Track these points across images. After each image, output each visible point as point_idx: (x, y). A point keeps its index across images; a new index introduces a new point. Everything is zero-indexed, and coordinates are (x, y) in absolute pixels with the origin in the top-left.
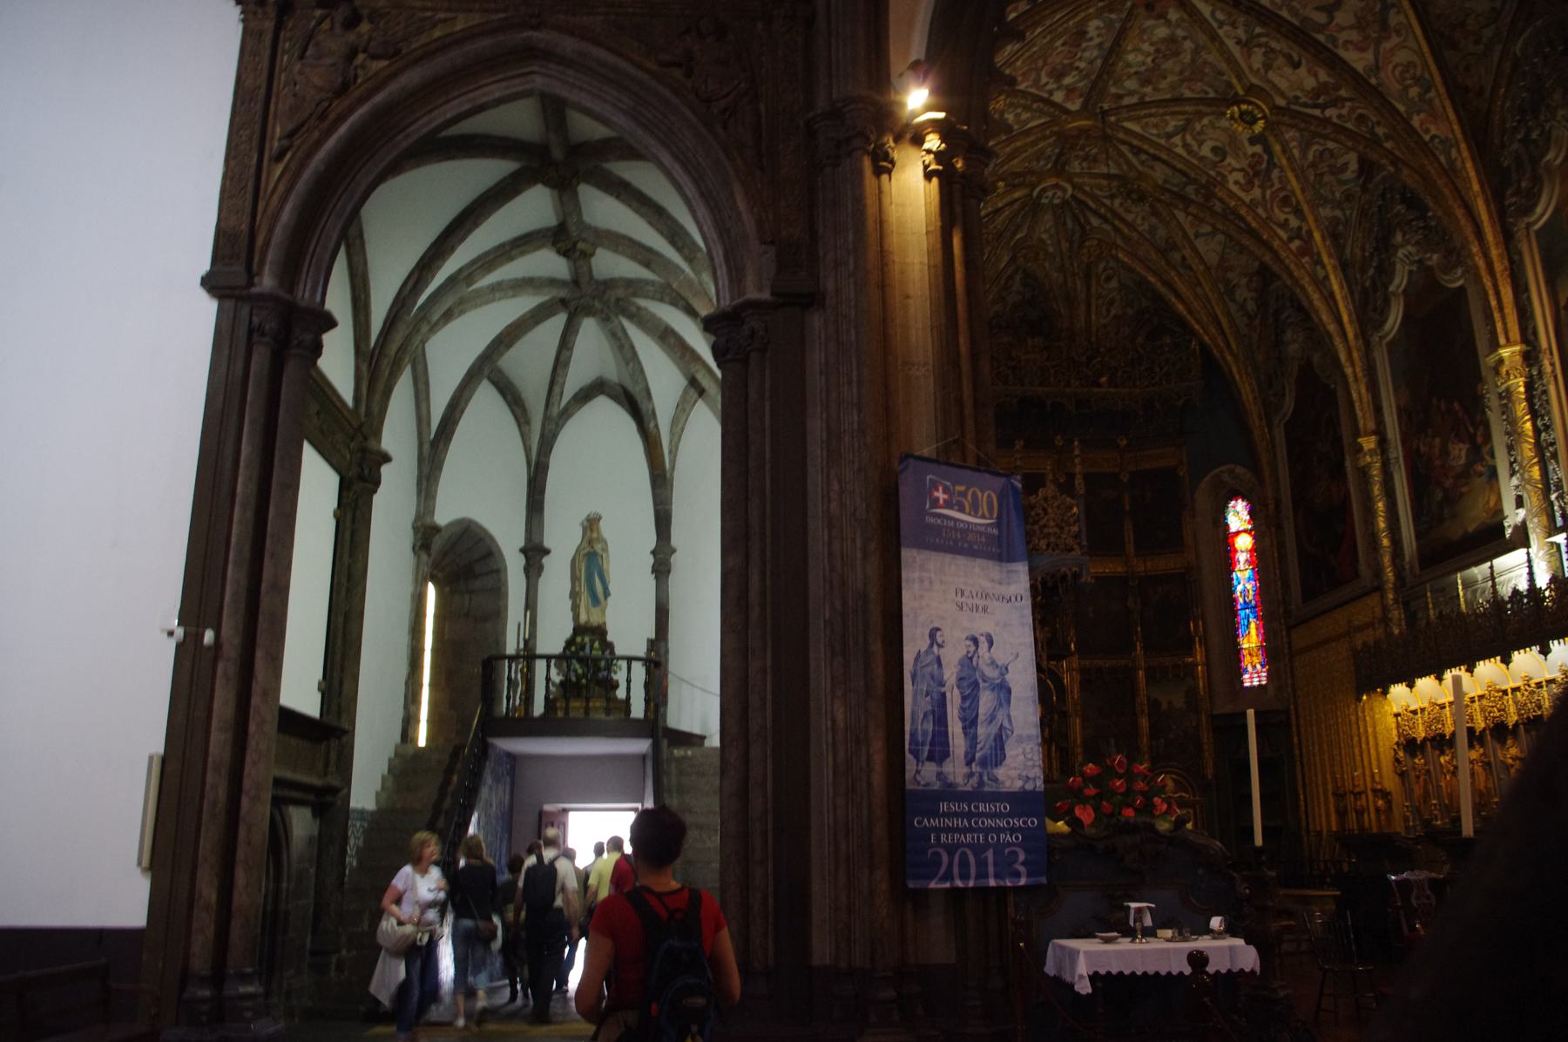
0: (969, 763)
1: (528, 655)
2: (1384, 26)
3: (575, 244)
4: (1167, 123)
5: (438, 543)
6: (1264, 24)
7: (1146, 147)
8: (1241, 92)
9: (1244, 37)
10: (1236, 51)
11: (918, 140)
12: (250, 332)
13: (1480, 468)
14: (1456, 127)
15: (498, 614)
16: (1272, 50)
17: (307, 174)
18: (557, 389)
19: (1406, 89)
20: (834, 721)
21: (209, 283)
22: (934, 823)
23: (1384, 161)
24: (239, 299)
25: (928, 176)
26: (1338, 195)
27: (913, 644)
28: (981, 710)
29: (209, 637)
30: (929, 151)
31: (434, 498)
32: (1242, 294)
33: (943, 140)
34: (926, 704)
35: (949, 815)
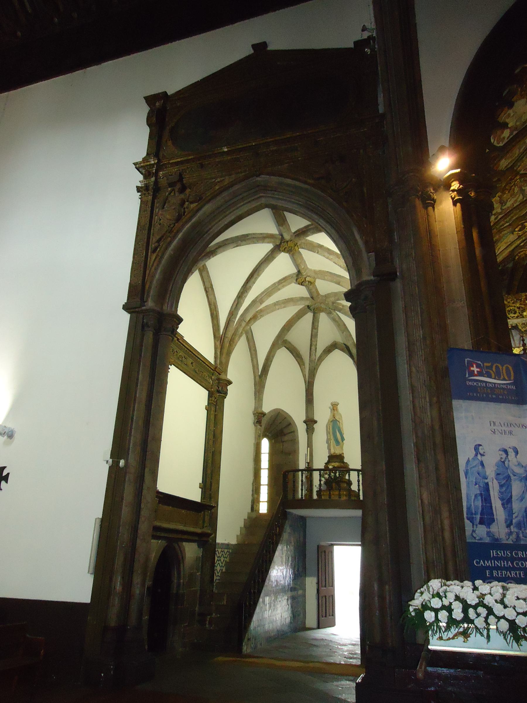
0: (508, 526)
1: (310, 470)
3: (305, 278)
5: (264, 421)
11: (447, 185)
12: (143, 327)
15: (295, 452)
17: (166, 256)
18: (313, 348)
21: (126, 308)
22: (488, 563)
24: (137, 312)
25: (455, 204)
27: (464, 454)
28: (514, 493)
29: (122, 463)
30: (453, 191)
31: (262, 400)
34: (476, 490)
35: (497, 559)
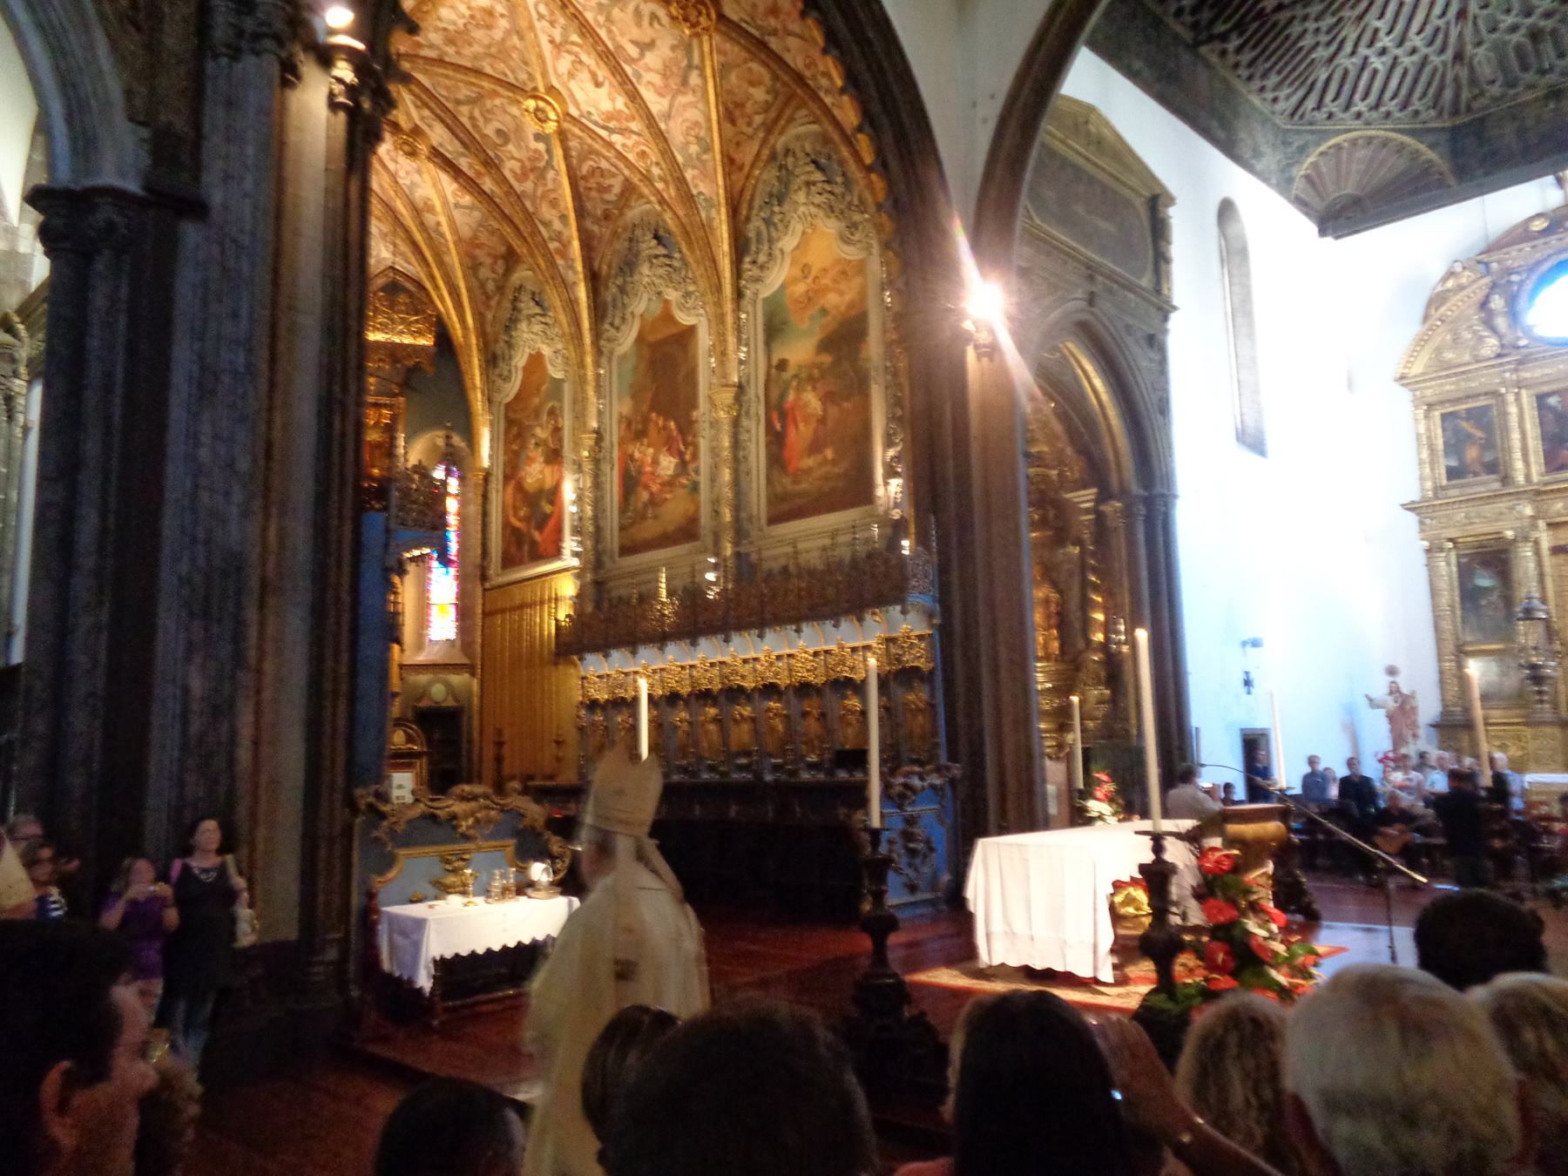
2: (685, 82)
4: (458, 88)
6: (582, 35)
7: (433, 105)
8: (542, 89)
9: (558, 39)
10: (547, 48)
13: (684, 481)
14: (721, 191)
16: (581, 62)
19: (688, 143)
20: (186, 690)
23: (653, 199)
25: (333, 105)
26: (599, 212)
30: (340, 81)
32: (484, 273)
33: (358, 71)
